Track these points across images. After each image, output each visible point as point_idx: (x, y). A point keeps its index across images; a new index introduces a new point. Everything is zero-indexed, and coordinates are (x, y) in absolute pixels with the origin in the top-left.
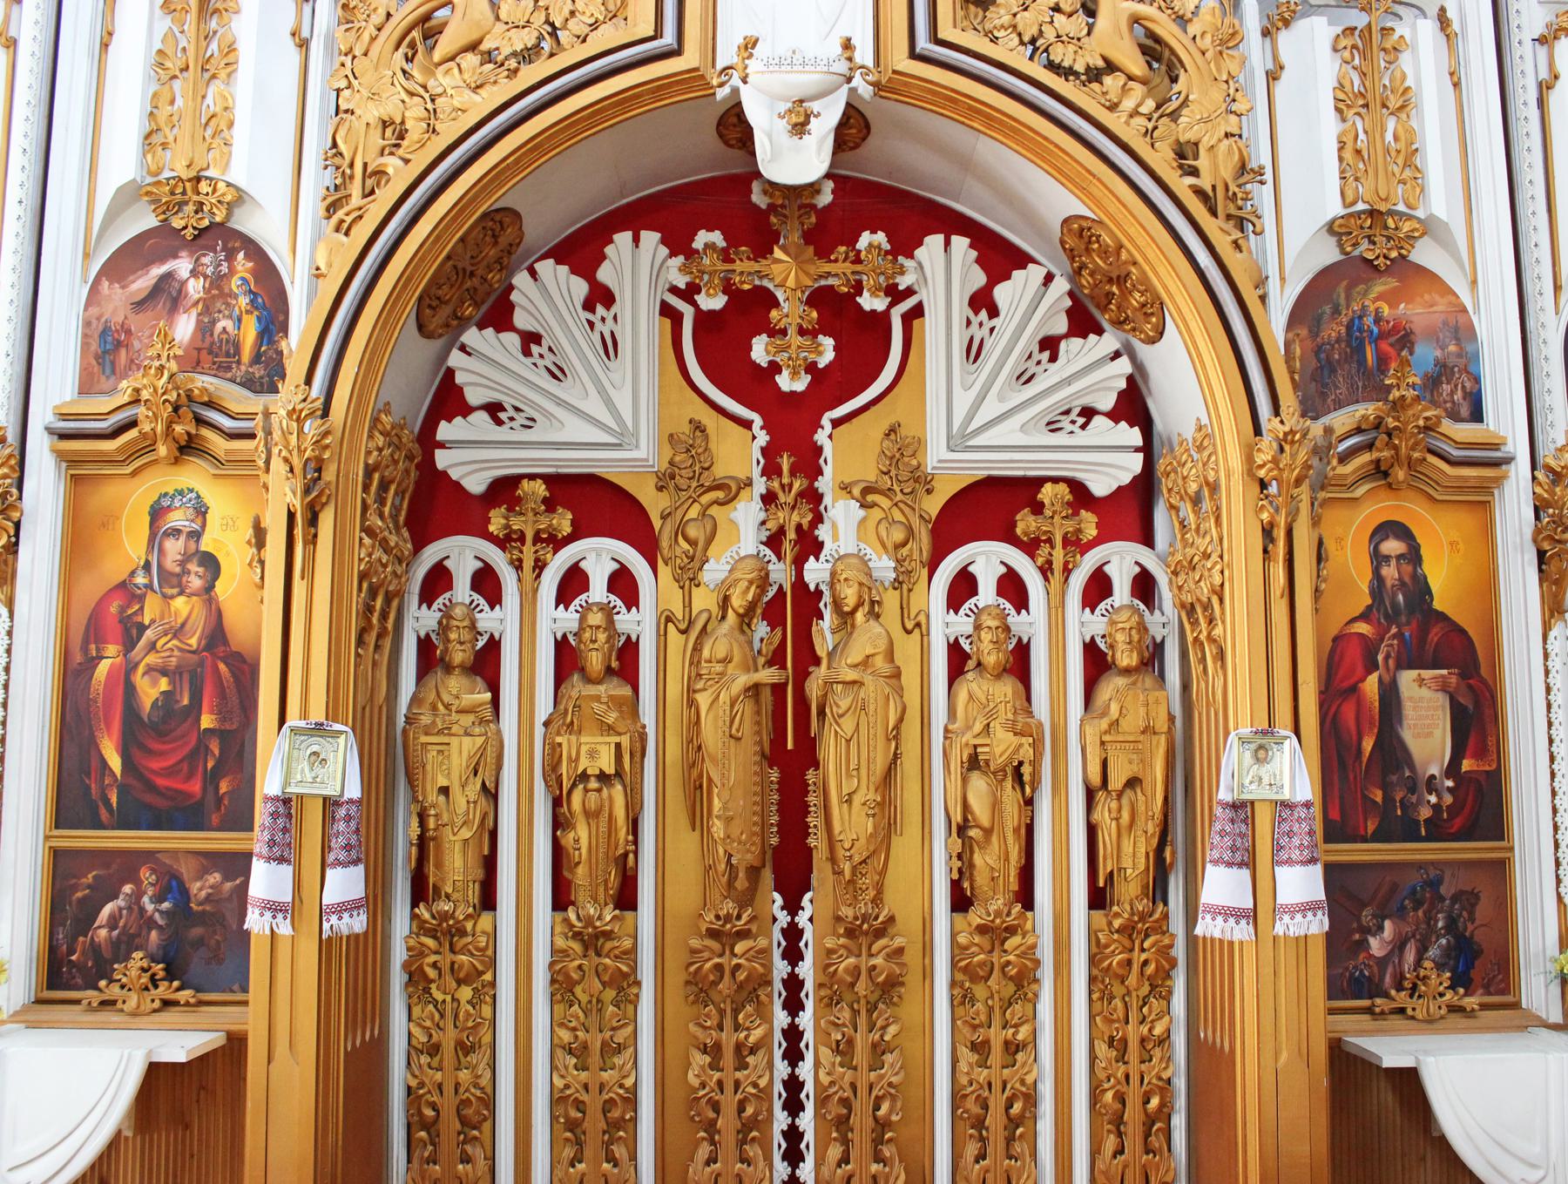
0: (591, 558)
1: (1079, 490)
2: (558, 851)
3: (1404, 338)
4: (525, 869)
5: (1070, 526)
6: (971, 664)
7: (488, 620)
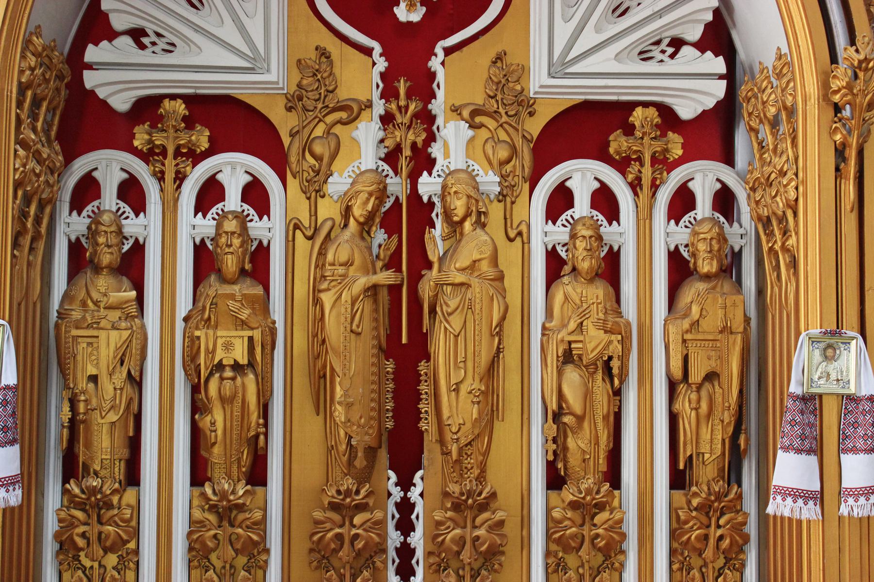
0: (227, 170)
1: (667, 113)
2: (196, 433)
4: (167, 447)
5: (658, 146)
6: (567, 269)
7: (133, 226)
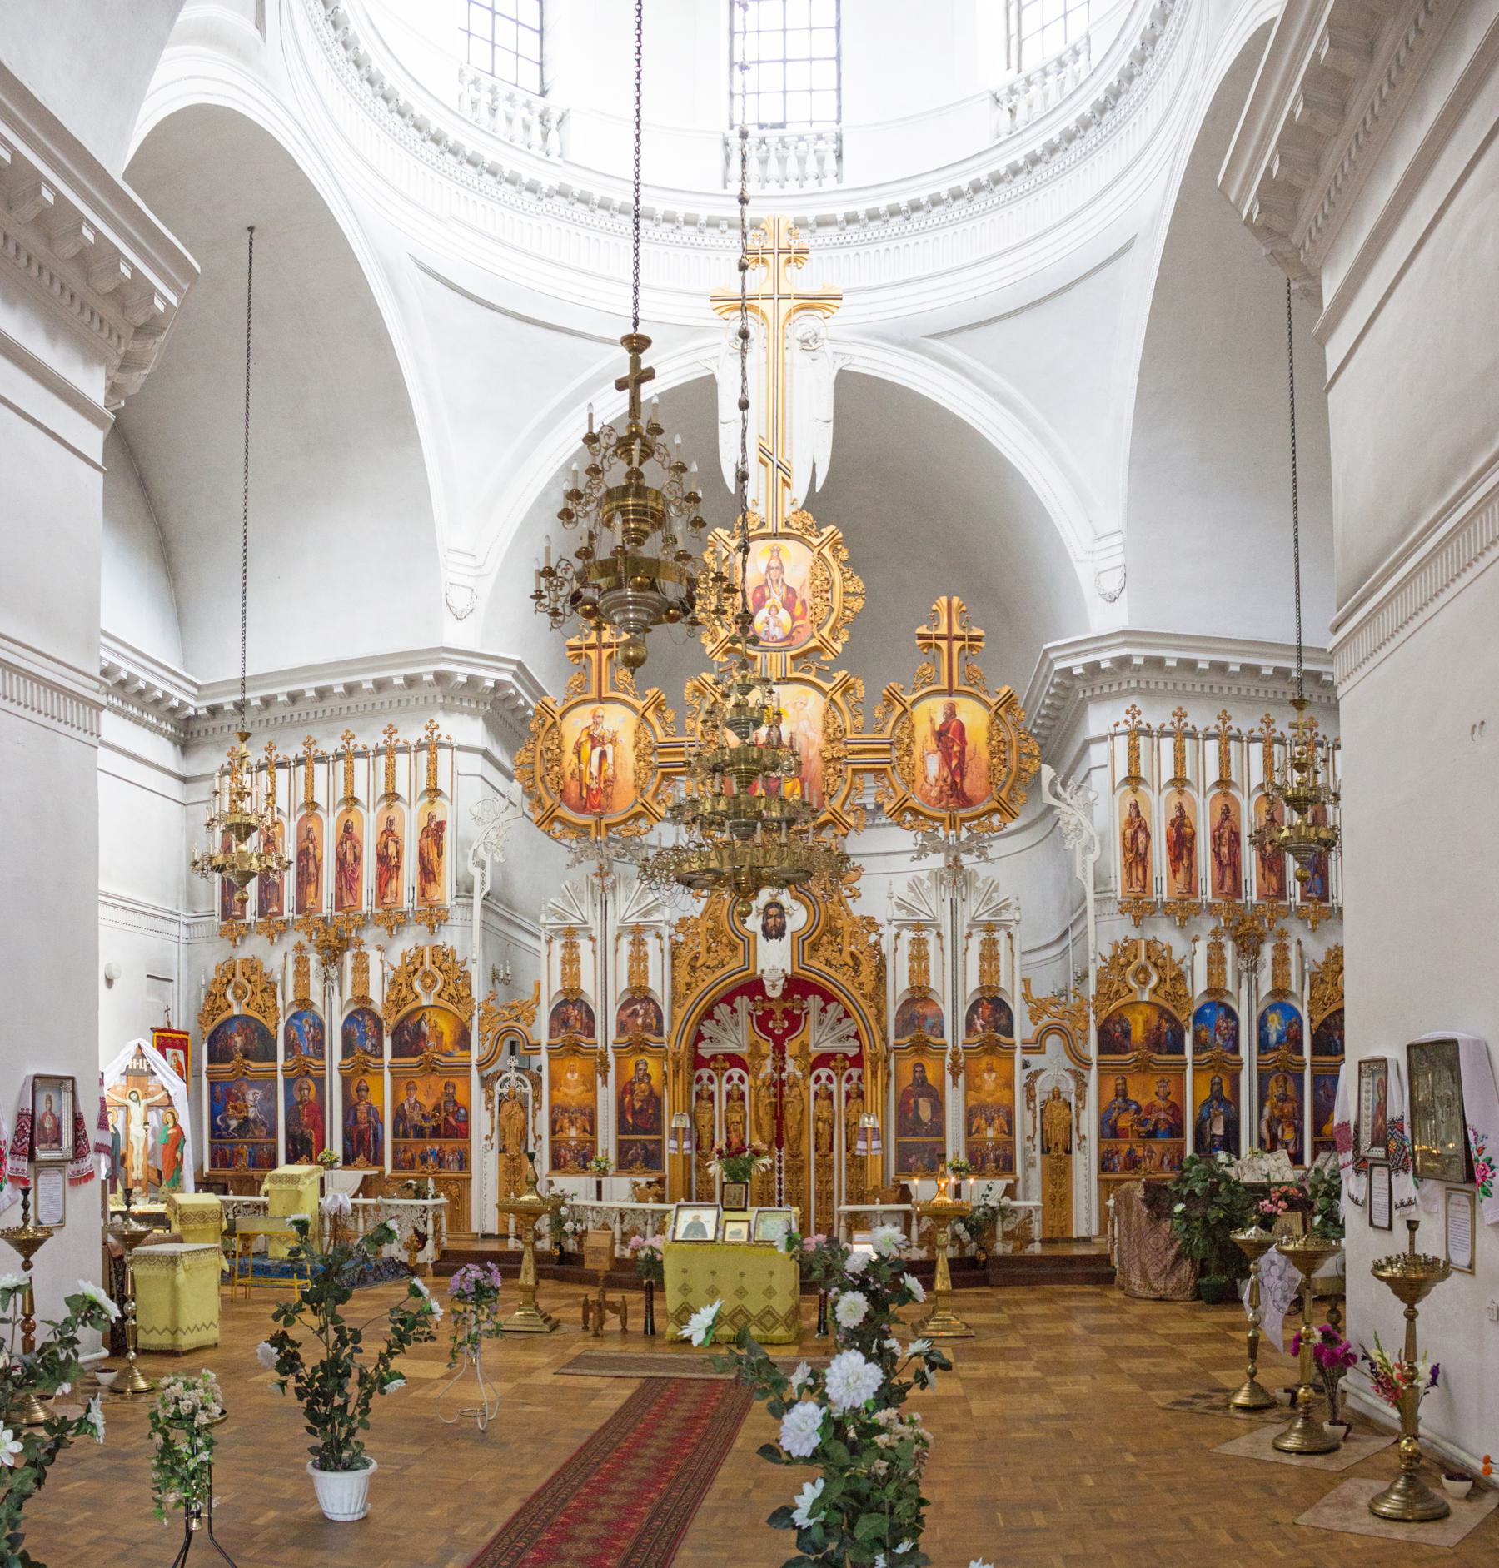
1: (845, 1055)
3: (925, 1017)
7: (711, 1087)
